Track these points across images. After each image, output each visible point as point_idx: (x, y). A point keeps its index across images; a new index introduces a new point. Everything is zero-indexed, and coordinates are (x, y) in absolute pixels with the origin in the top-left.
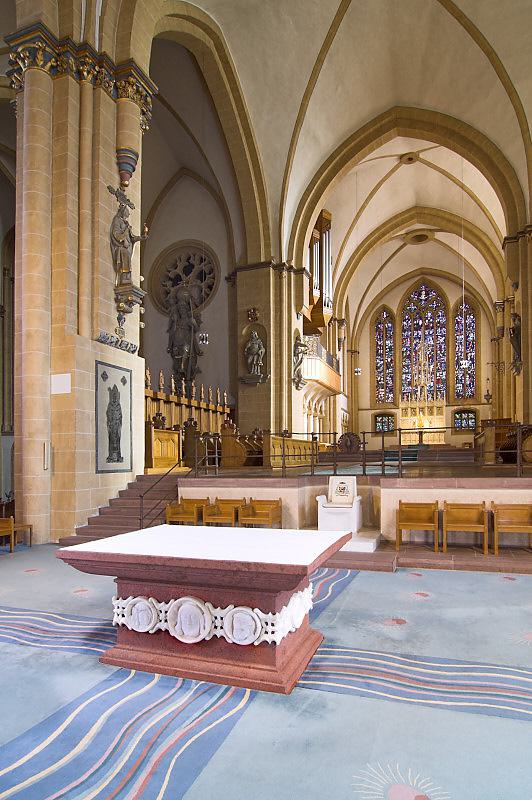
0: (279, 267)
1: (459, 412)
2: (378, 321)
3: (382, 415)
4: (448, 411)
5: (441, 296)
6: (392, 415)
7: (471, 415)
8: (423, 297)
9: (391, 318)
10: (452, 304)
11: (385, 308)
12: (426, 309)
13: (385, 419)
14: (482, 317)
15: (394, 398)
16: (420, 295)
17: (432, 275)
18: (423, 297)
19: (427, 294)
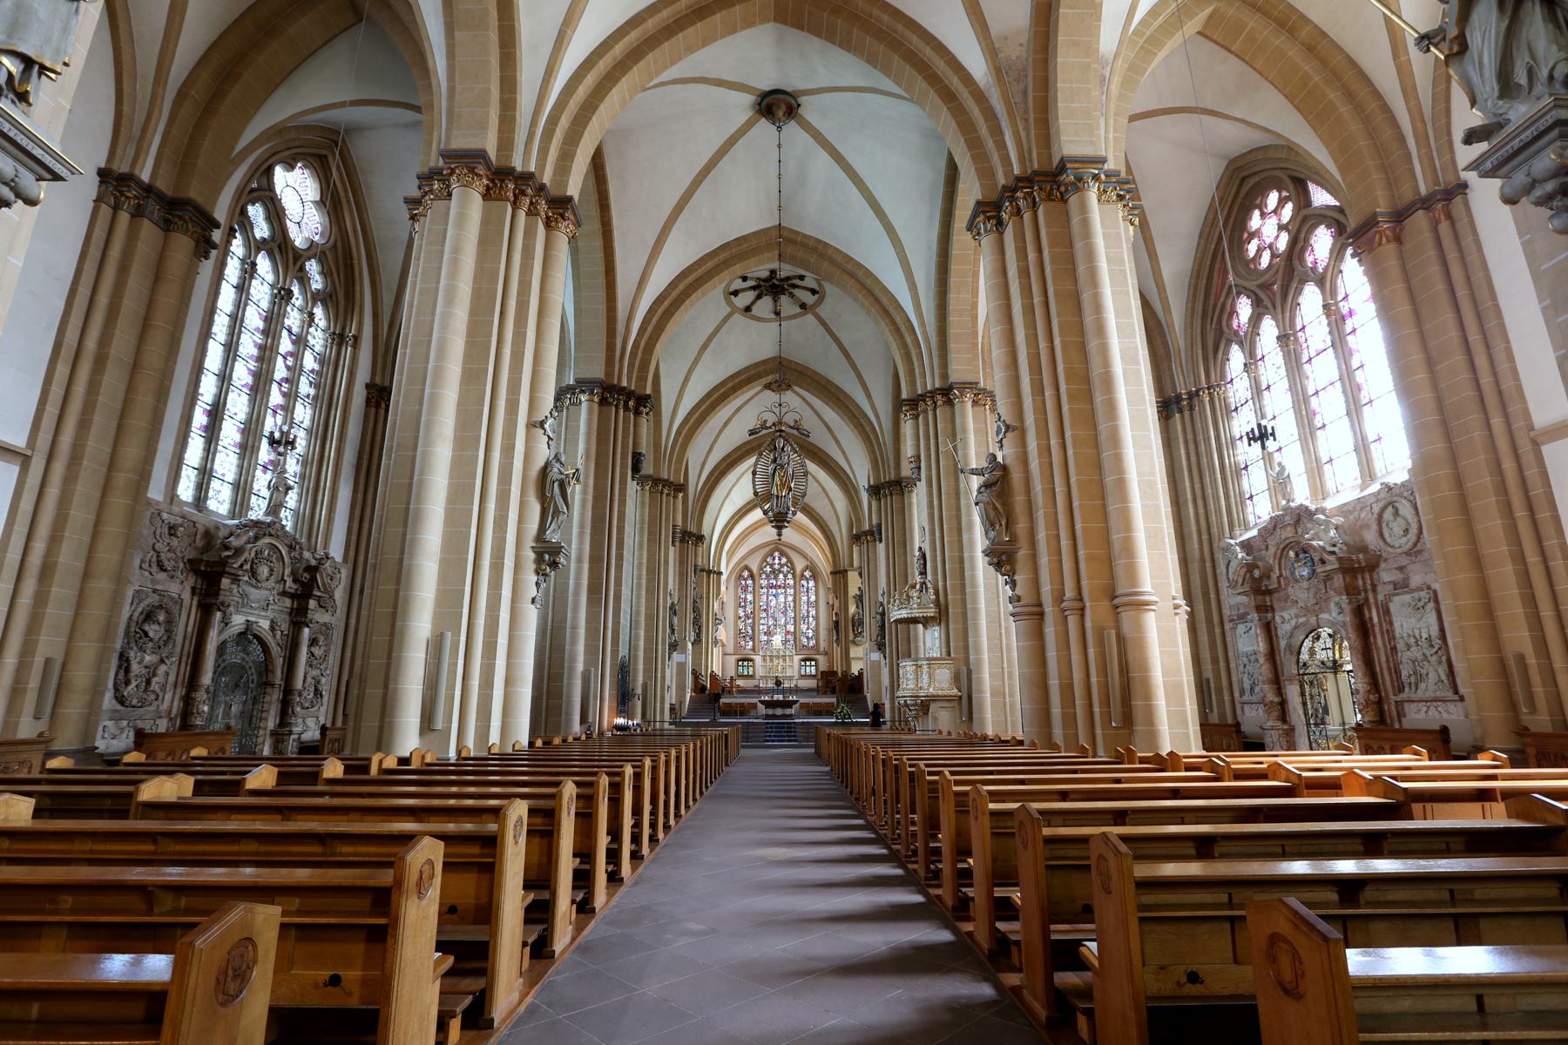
0: (709, 572)
1: (805, 660)
2: (740, 576)
3: (743, 660)
4: (797, 658)
5: (790, 560)
6: (751, 660)
7: (813, 663)
8: (777, 561)
9: (752, 576)
10: (798, 570)
11: (746, 568)
12: (780, 572)
13: (746, 663)
14: (820, 583)
15: (754, 646)
16: (774, 559)
17: (786, 546)
18: (777, 561)
19: (780, 559)
